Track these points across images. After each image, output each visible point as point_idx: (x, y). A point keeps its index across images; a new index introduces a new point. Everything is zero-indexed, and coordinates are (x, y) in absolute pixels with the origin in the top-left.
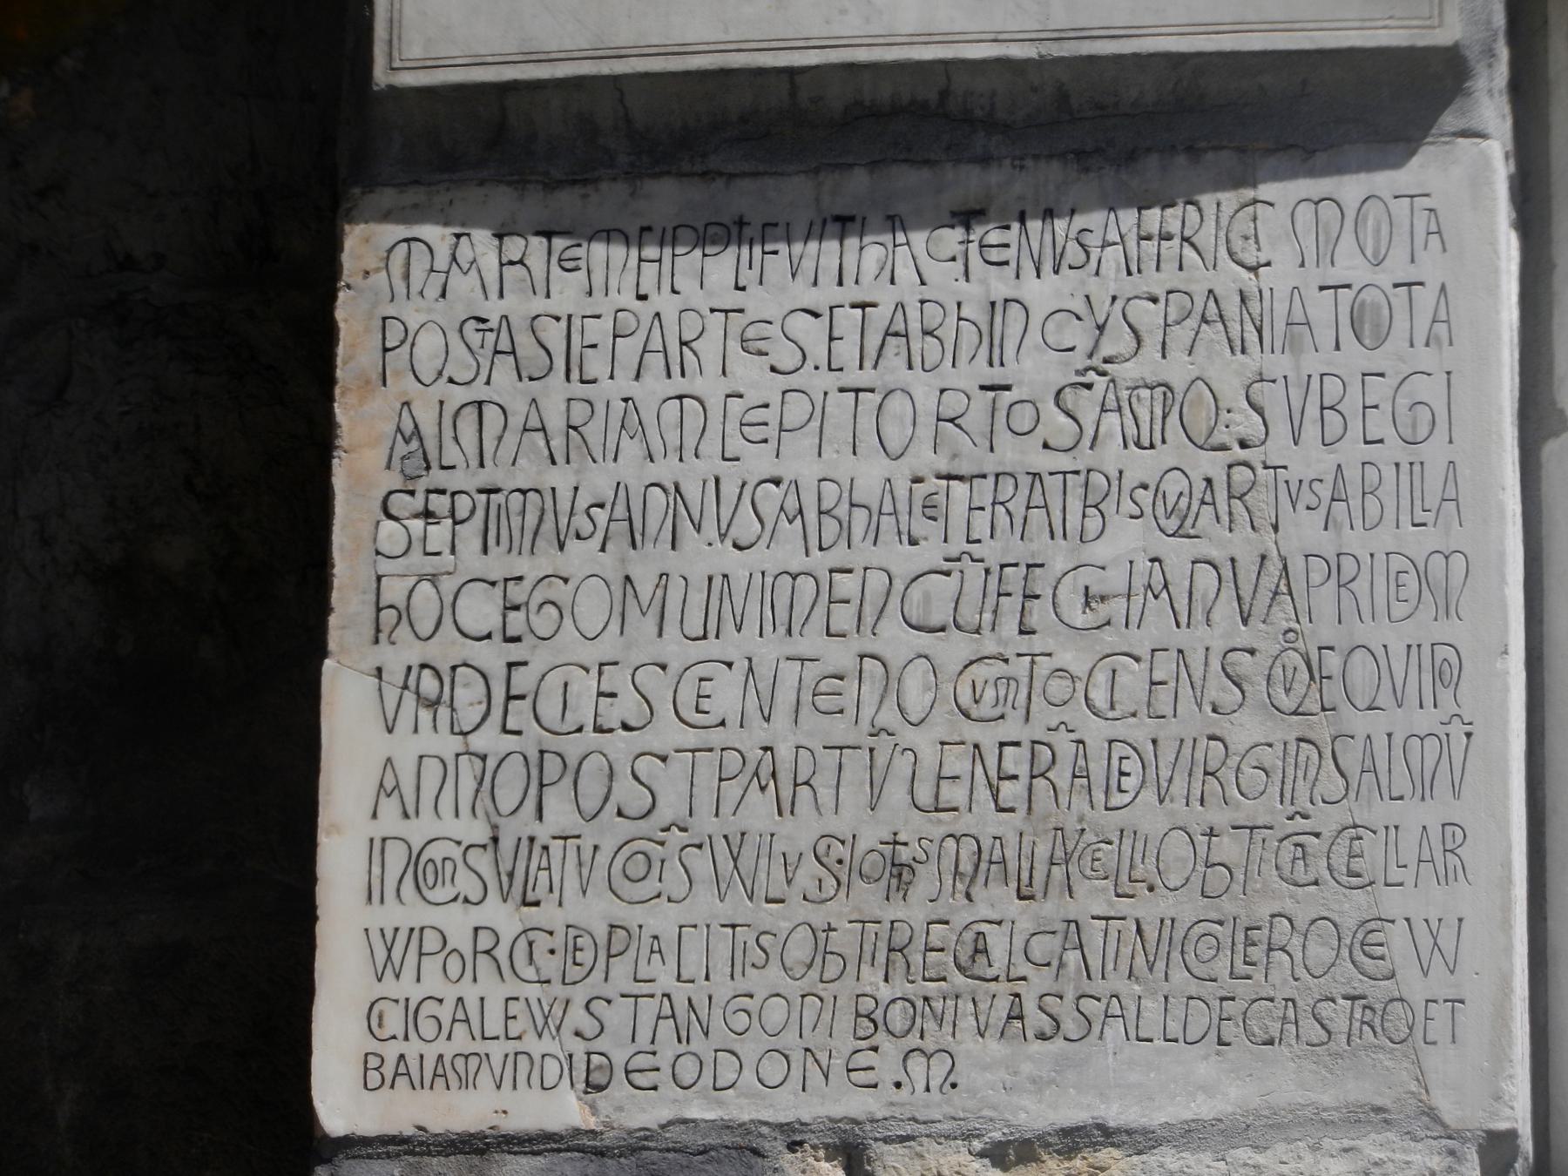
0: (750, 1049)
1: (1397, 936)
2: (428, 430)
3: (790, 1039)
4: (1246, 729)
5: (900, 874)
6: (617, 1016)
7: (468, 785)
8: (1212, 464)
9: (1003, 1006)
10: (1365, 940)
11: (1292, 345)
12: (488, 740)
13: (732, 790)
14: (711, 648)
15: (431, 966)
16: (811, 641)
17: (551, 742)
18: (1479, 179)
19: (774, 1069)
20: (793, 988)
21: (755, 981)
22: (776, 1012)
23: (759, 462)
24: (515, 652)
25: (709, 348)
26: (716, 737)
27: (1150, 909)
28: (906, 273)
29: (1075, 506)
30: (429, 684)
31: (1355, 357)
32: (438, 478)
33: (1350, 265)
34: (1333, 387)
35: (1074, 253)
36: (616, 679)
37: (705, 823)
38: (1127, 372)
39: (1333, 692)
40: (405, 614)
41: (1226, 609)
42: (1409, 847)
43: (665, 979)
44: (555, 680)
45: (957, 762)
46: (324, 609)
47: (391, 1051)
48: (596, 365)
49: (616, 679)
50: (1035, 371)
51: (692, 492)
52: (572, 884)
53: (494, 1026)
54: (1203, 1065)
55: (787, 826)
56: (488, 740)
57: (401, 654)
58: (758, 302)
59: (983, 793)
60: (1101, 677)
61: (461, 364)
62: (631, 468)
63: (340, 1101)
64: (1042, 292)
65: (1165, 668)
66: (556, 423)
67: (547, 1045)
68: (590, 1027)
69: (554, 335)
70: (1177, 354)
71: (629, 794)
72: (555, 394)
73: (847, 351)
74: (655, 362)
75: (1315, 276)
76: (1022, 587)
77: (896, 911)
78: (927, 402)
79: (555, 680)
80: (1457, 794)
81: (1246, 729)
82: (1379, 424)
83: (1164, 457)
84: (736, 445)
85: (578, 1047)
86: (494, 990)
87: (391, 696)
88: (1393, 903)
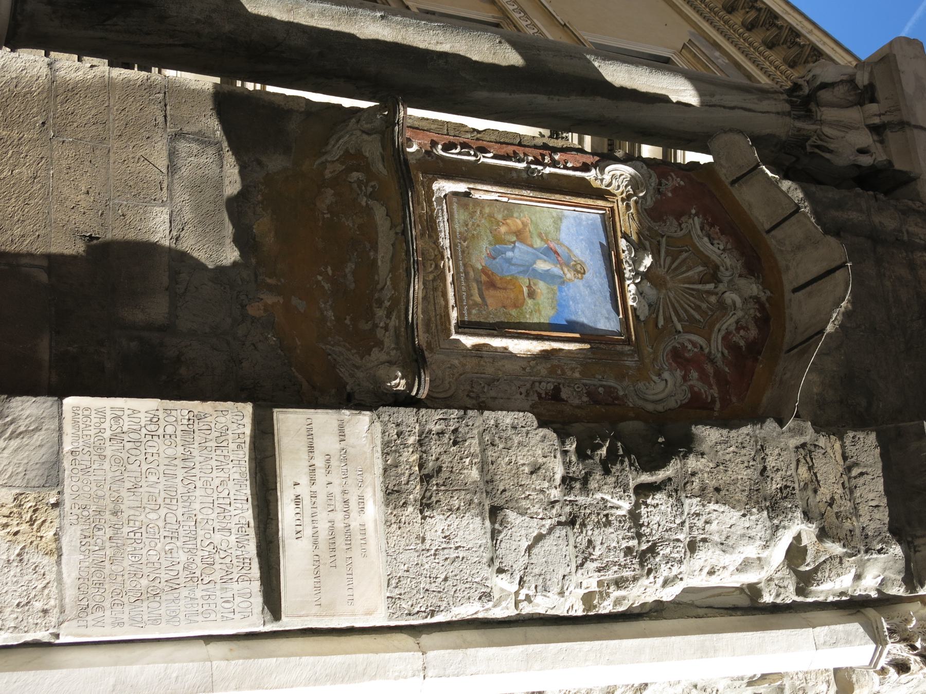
0: (79, 483)
1: (101, 614)
2: (206, 420)
3: (81, 492)
4: (144, 582)
5: (115, 513)
6: (87, 457)
7: (134, 427)
8: (198, 574)
9: (87, 534)
10: (99, 607)
11: (222, 589)
12: (144, 431)
13: (133, 480)
14: (162, 475)
15: (98, 420)
16: (163, 495)
17: (143, 444)
18: (254, 625)
19: (75, 488)
20: (92, 492)
21: (93, 486)
22: (87, 489)
23: (199, 484)
24: (161, 437)
26: (144, 476)
27: (107, 563)
28: (237, 512)
29: (190, 546)
30: (155, 420)
31: (219, 601)
32: (196, 421)
33: (238, 600)
34: (213, 597)
35: (240, 545)
37: (126, 474)
38: (217, 556)
39: (151, 599)
40: (169, 415)
41: (168, 577)
42: (119, 616)
44: (155, 444)
45: (137, 524)
46: (170, 400)
47: (80, 412)
48: (218, 452)
50: (217, 538)
51: (193, 471)
52: (113, 448)
53: (85, 433)
54: (75, 574)
55: (125, 490)
56: (144, 431)
57: (161, 414)
58: (231, 483)
59: (131, 529)
60: (155, 553)
61: (219, 426)
62: (198, 459)
63: (70, 402)
64: (233, 538)
65: (157, 565)
66: (207, 444)
67: (81, 444)
68: (84, 452)
69: (224, 444)
70: (220, 566)
71: (133, 459)
72: (213, 444)
73: (221, 501)
74: (219, 464)
75: (235, 592)
76: (174, 537)
77: (108, 513)
78: (211, 517)
79: (155, 444)
80: (131, 625)
81: (144, 582)
82: (206, 607)
83: (200, 564)
84: (202, 479)
85: (80, 449)
86: (92, 433)
87: (153, 412)
88: (108, 613)
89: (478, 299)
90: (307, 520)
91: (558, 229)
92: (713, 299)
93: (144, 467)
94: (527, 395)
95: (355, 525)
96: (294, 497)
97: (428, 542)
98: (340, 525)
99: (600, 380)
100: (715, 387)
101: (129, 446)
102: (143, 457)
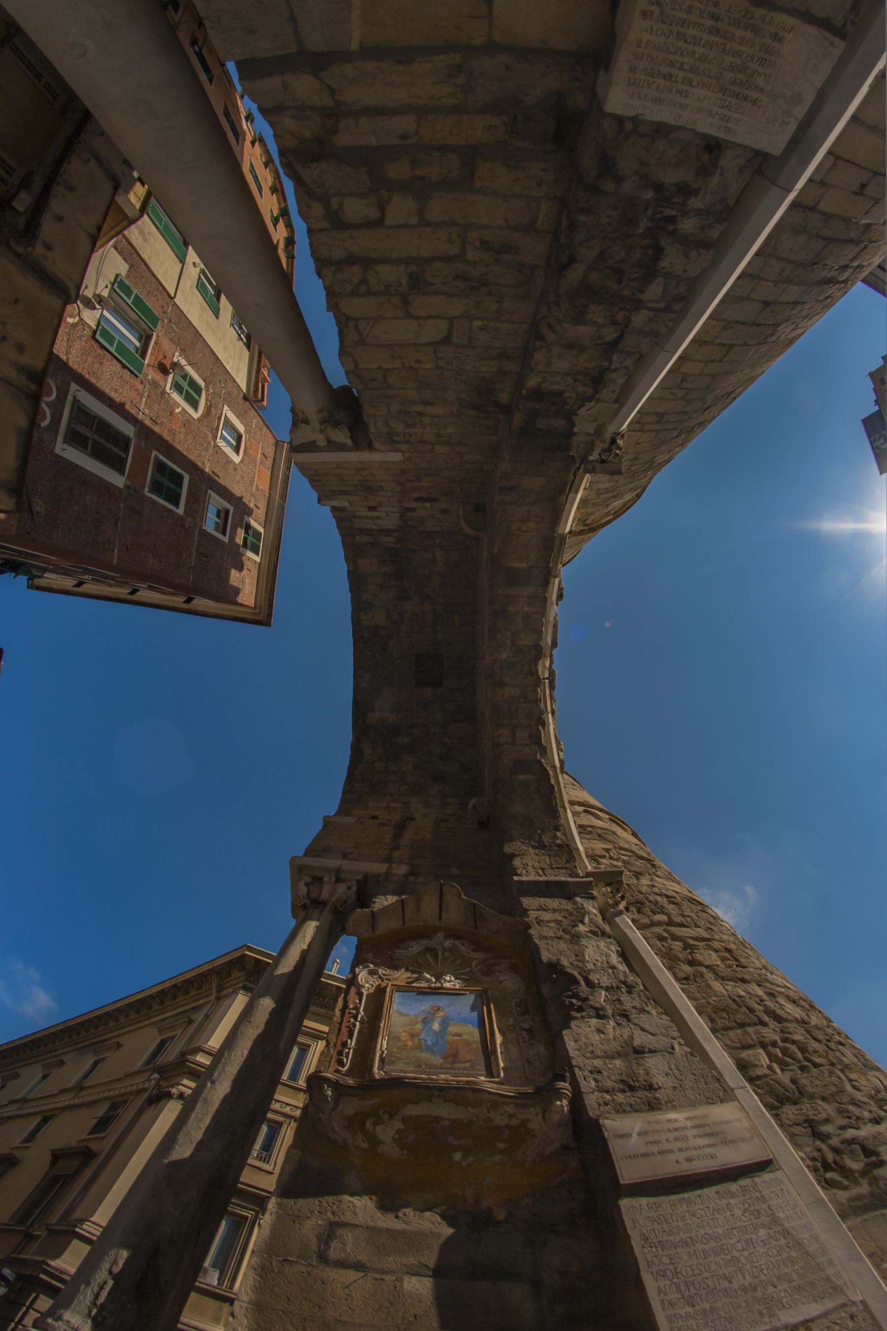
12: (675, 1280)
22: (744, 1316)
25: (687, 1216)
36: (694, 1267)
40: (653, 1262)
43: (723, 1314)
48: (670, 1221)
49: (694, 1267)
56: (675, 1280)
57: (654, 1269)
62: (682, 1235)
66: (667, 1229)
72: (665, 1226)
89: (468, 1065)
90: (699, 1152)
91: (407, 1015)
92: (447, 954)
93: (706, 1275)
95: (689, 1124)
96: (688, 1163)
97: (675, 1085)
98: (695, 1132)
101: (693, 1291)
102: (698, 1278)
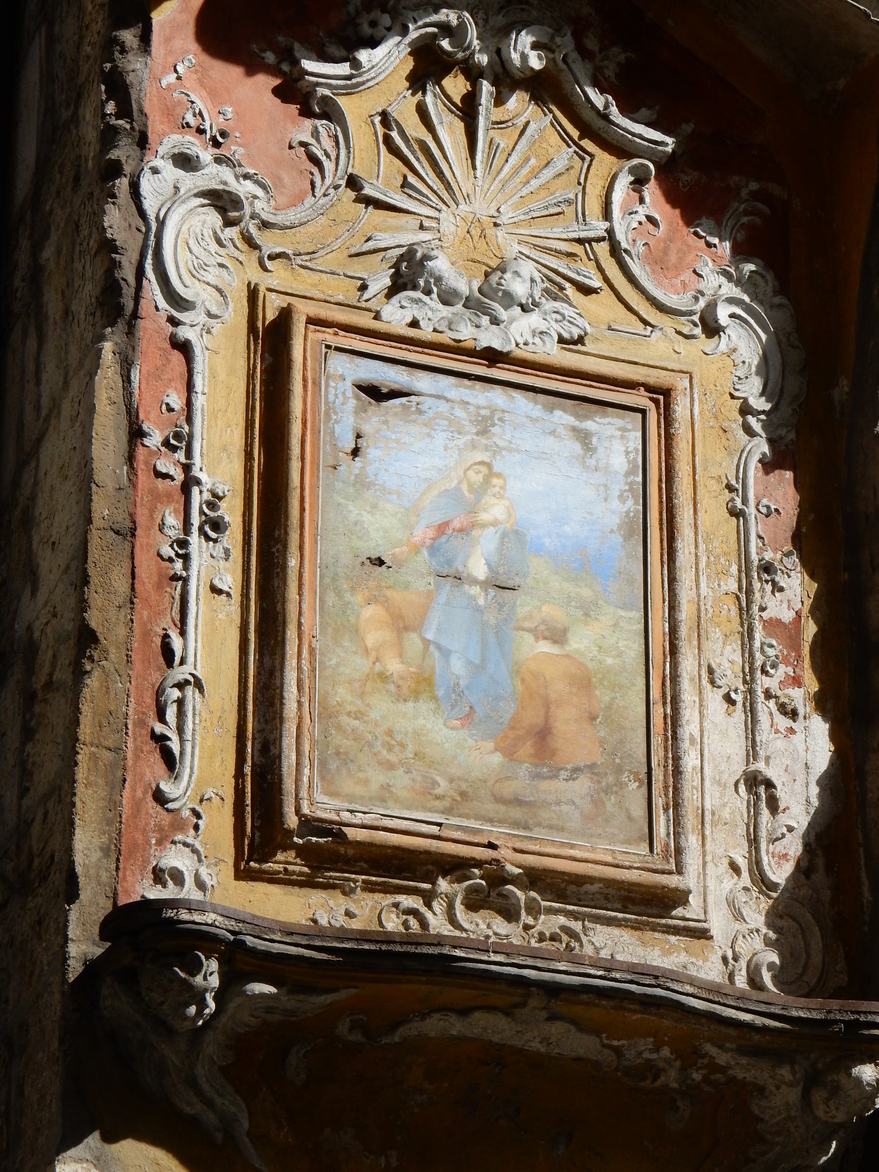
94: (793, 714)
99: (745, 501)
100: (735, 179)
